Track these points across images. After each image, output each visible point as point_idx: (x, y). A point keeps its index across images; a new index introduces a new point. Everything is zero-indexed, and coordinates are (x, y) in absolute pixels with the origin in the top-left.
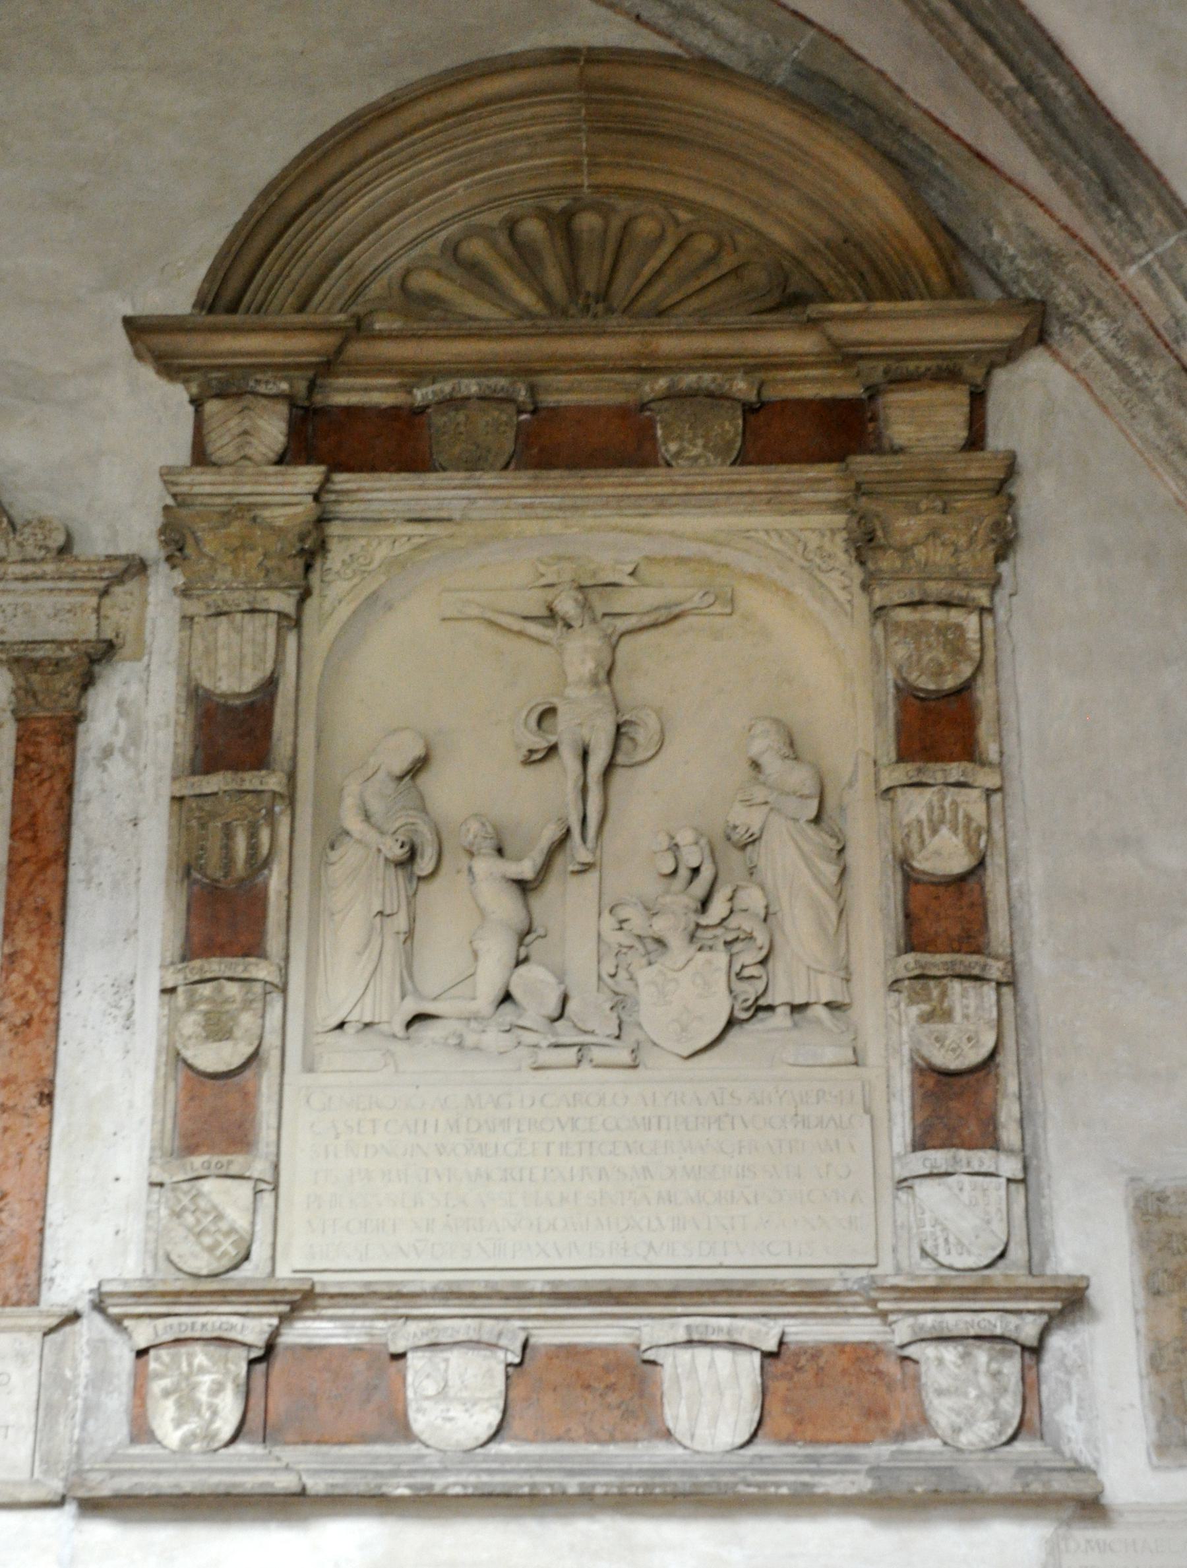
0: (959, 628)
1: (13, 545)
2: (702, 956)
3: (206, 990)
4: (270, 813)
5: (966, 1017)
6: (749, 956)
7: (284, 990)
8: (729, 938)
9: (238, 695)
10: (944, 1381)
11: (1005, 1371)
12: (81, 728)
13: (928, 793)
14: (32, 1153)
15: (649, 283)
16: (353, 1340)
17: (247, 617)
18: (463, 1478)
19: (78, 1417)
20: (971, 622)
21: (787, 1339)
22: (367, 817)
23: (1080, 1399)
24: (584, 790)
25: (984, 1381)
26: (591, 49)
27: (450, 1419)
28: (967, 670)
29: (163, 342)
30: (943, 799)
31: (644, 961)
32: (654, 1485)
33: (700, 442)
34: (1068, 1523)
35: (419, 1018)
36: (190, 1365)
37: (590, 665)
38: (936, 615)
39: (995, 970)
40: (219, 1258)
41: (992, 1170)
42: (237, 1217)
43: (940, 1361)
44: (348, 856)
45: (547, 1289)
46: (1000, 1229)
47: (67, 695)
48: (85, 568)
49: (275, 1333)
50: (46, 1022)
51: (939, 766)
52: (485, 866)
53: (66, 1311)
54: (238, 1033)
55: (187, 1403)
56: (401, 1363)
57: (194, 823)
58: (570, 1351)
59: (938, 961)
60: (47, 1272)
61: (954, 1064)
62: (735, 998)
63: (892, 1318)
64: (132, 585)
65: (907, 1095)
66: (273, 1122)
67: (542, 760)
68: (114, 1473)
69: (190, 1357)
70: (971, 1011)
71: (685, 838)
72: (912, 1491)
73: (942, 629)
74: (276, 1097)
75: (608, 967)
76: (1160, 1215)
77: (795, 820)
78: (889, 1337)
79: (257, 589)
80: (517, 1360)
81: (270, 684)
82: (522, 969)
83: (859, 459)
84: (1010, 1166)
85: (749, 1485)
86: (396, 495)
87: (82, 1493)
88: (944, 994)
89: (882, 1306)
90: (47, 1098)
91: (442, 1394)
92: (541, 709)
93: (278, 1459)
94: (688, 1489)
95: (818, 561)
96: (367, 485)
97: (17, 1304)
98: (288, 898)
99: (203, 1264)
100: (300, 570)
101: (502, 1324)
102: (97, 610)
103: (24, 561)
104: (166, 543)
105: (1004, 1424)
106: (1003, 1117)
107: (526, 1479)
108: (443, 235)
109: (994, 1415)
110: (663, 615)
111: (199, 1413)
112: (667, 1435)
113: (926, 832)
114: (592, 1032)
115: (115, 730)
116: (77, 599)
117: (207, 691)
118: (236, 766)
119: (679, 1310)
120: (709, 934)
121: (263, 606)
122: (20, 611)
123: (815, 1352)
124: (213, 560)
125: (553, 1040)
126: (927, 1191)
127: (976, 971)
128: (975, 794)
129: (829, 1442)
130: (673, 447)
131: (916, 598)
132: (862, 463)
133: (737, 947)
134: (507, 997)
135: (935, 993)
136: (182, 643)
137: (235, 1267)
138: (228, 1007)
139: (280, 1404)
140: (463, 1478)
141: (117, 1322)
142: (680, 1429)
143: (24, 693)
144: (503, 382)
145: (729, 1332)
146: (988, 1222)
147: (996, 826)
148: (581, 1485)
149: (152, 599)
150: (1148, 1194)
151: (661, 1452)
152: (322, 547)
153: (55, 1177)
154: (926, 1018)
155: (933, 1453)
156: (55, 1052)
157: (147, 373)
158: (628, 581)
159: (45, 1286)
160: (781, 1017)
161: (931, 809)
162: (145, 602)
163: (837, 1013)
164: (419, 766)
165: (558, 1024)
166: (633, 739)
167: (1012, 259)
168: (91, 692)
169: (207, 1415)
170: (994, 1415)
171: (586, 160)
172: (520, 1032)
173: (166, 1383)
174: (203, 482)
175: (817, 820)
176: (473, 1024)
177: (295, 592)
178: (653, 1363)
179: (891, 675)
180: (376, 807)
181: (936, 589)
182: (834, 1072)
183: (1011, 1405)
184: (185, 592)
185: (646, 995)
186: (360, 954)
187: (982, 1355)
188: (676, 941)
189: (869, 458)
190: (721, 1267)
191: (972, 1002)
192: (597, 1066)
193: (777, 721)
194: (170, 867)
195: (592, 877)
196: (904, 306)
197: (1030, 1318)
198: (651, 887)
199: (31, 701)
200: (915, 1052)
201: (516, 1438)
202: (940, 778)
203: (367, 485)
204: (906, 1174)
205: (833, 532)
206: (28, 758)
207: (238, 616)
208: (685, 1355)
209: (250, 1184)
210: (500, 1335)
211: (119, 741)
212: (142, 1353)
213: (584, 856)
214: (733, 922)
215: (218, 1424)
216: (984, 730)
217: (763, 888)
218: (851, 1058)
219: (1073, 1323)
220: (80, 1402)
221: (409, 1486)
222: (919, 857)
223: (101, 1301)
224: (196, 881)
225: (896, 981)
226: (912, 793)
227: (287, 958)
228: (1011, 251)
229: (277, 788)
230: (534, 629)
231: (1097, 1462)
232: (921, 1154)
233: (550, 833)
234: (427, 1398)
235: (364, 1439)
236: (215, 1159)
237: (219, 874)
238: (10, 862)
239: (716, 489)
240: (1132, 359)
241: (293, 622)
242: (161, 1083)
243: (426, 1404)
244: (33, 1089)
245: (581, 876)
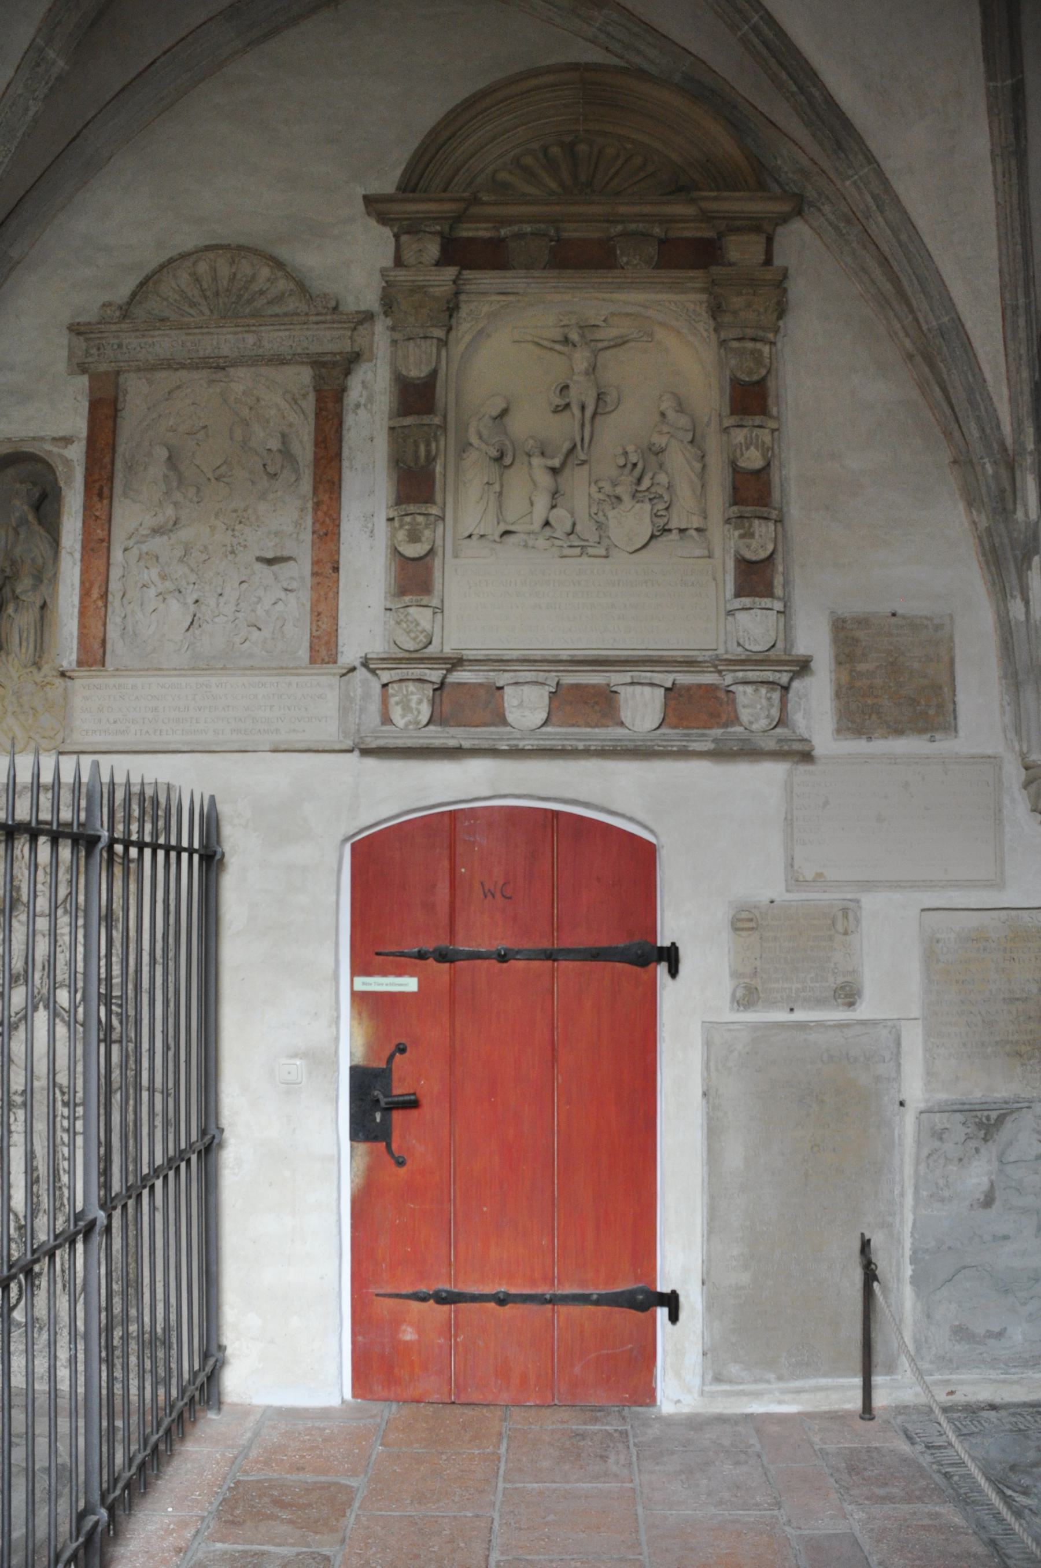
0: (760, 352)
1: (312, 306)
2: (638, 506)
3: (408, 519)
4: (435, 435)
5: (761, 536)
6: (661, 506)
7: (443, 519)
8: (652, 496)
9: (419, 378)
10: (746, 702)
11: (774, 697)
12: (345, 394)
13: (745, 431)
14: (331, 595)
15: (612, 179)
16: (479, 681)
17: (423, 340)
18: (531, 742)
19: (357, 713)
20: (766, 349)
21: (676, 682)
22: (481, 437)
23: (805, 710)
24: (583, 425)
25: (764, 701)
26: (587, 64)
27: (524, 716)
28: (763, 372)
29: (380, 207)
30: (752, 432)
31: (611, 508)
32: (617, 746)
33: (638, 257)
34: (797, 763)
35: (507, 533)
36: (407, 691)
37: (585, 364)
38: (750, 345)
39: (774, 514)
40: (418, 643)
41: (770, 607)
42: (426, 624)
43: (745, 693)
44: (472, 456)
45: (569, 658)
46: (773, 634)
47: (339, 378)
48: (345, 317)
49: (445, 677)
50: (334, 534)
51: (750, 417)
52: (536, 461)
53: (350, 666)
54: (423, 539)
55: (406, 708)
56: (501, 691)
57: (400, 440)
58: (577, 687)
59: (748, 510)
60: (340, 649)
61: (754, 558)
62: (654, 525)
63: (724, 673)
64: (366, 325)
65: (733, 574)
66: (441, 581)
67: (562, 411)
68: (377, 738)
69: (407, 687)
70: (763, 534)
71: (630, 449)
72: (731, 749)
73: (752, 352)
74: (441, 570)
75: (594, 510)
76: (843, 628)
77: (682, 441)
78: (722, 682)
79: (428, 327)
80: (554, 690)
81: (434, 374)
82: (555, 511)
83: (714, 268)
84: (778, 606)
85: (659, 746)
86: (492, 281)
87: (362, 746)
88: (750, 526)
89: (720, 668)
90: (336, 569)
91: (521, 705)
92: (562, 386)
93: (448, 733)
94: (632, 747)
95: (694, 317)
96: (478, 276)
97: (328, 663)
98: (445, 475)
99: (411, 646)
100: (447, 317)
101: (547, 674)
102: (351, 338)
103: (317, 314)
104: (384, 305)
105: (772, 721)
106: (776, 582)
107: (560, 743)
108: (512, 154)
109: (768, 716)
110: (620, 341)
111: (412, 712)
112: (622, 724)
113: (744, 448)
114: (587, 541)
115: (361, 396)
116: (342, 332)
117: (404, 376)
118: (419, 413)
119: (628, 668)
120: (640, 495)
121: (431, 335)
122: (315, 338)
123: (689, 688)
124: (405, 312)
125: (569, 544)
126: (741, 616)
127: (765, 515)
128: (767, 431)
129: (694, 728)
130: (625, 259)
131: (740, 336)
132: (715, 270)
133: (655, 501)
134: (547, 523)
135: (747, 525)
136: (391, 352)
137: (425, 647)
138: (418, 527)
139: (447, 709)
140: (531, 742)
141: (373, 672)
142: (627, 722)
143: (318, 379)
144: (543, 226)
145: (650, 679)
146: (768, 631)
147: (776, 447)
148: (585, 745)
149: (376, 332)
150: (838, 619)
151: (619, 732)
152: (457, 307)
153: (341, 606)
154: (742, 536)
155: (741, 733)
156: (339, 548)
157: (373, 223)
158: (603, 324)
159: (339, 655)
160: (675, 535)
161: (746, 439)
162: (373, 334)
163: (701, 533)
164: (504, 412)
165: (572, 537)
166: (605, 402)
167: (786, 173)
168: (349, 377)
169: (416, 713)
170: (768, 716)
171: (581, 118)
172: (553, 540)
173: (397, 699)
174: (401, 275)
175: (692, 442)
176: (532, 536)
177: (445, 328)
178: (616, 692)
179: (728, 373)
180: (485, 433)
181: (750, 332)
182: (700, 561)
183: (775, 712)
184: (393, 329)
185: (612, 523)
186: (478, 502)
187: (763, 691)
188: (626, 498)
189: (719, 268)
190: (646, 649)
191: (764, 529)
192: (590, 556)
193: (672, 393)
194: (389, 461)
195: (586, 467)
196: (737, 194)
197: (785, 674)
198: (614, 472)
199: (322, 381)
200: (737, 552)
201: (554, 725)
202: (750, 423)
203: (478, 276)
204: (732, 608)
205: (701, 303)
206: (321, 409)
207: (419, 340)
208: (630, 689)
209: (432, 609)
210: (546, 679)
211: (363, 401)
212: (385, 686)
213: (582, 456)
214: (653, 490)
215: (420, 717)
216: (771, 401)
217: (667, 474)
218: (706, 553)
219: (803, 677)
220: (358, 707)
221: (508, 745)
222: (740, 460)
223: (366, 662)
224: (401, 468)
225: (729, 519)
226: (738, 430)
227: (444, 504)
228: (786, 169)
229: (438, 423)
230: (558, 347)
231: (810, 736)
232: (739, 600)
233: (567, 446)
234: (514, 707)
235: (485, 725)
236: (414, 598)
237: (412, 464)
238: (315, 458)
239: (645, 280)
240: (842, 225)
241: (443, 343)
242: (388, 562)
243: (514, 710)
244: (329, 565)
245: (579, 467)
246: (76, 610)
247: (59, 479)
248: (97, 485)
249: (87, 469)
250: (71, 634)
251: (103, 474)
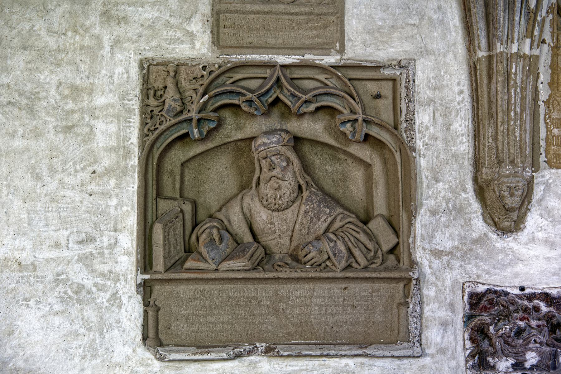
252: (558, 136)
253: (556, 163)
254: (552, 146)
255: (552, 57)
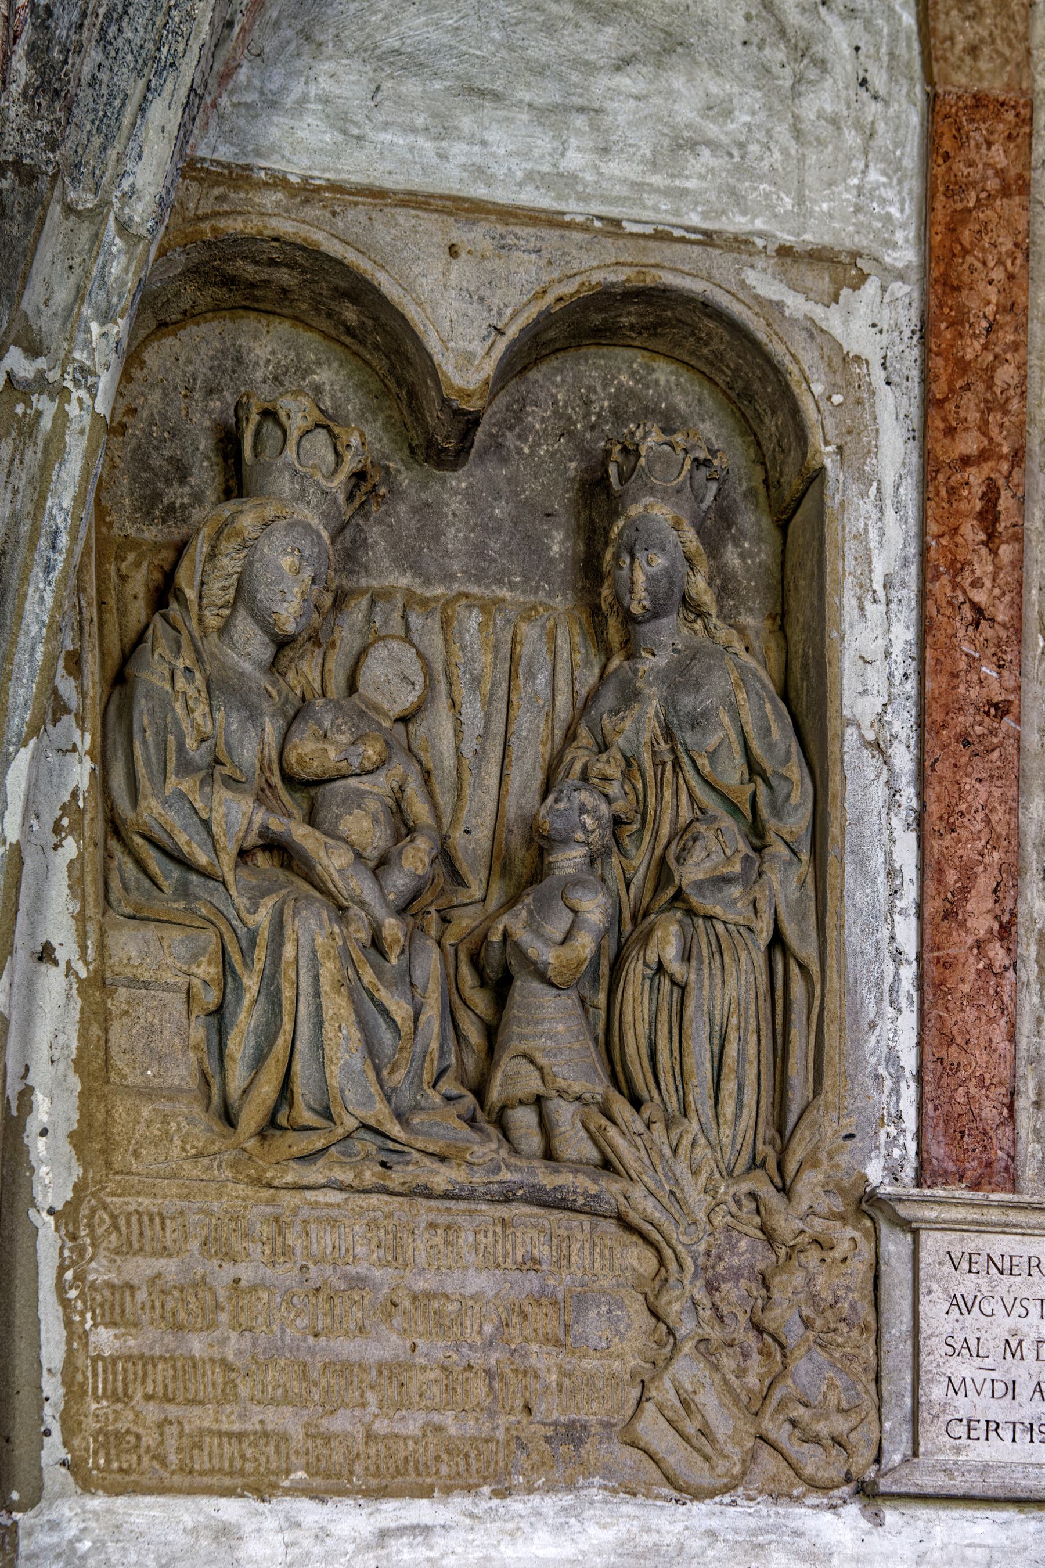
246: (908, 973)
247: (816, 438)
248: (975, 477)
249: (929, 403)
250: (892, 1059)
251: (994, 432)
252: (114, 1360)
253: (107, 1469)
254: (89, 1399)
255: (84, 1023)
